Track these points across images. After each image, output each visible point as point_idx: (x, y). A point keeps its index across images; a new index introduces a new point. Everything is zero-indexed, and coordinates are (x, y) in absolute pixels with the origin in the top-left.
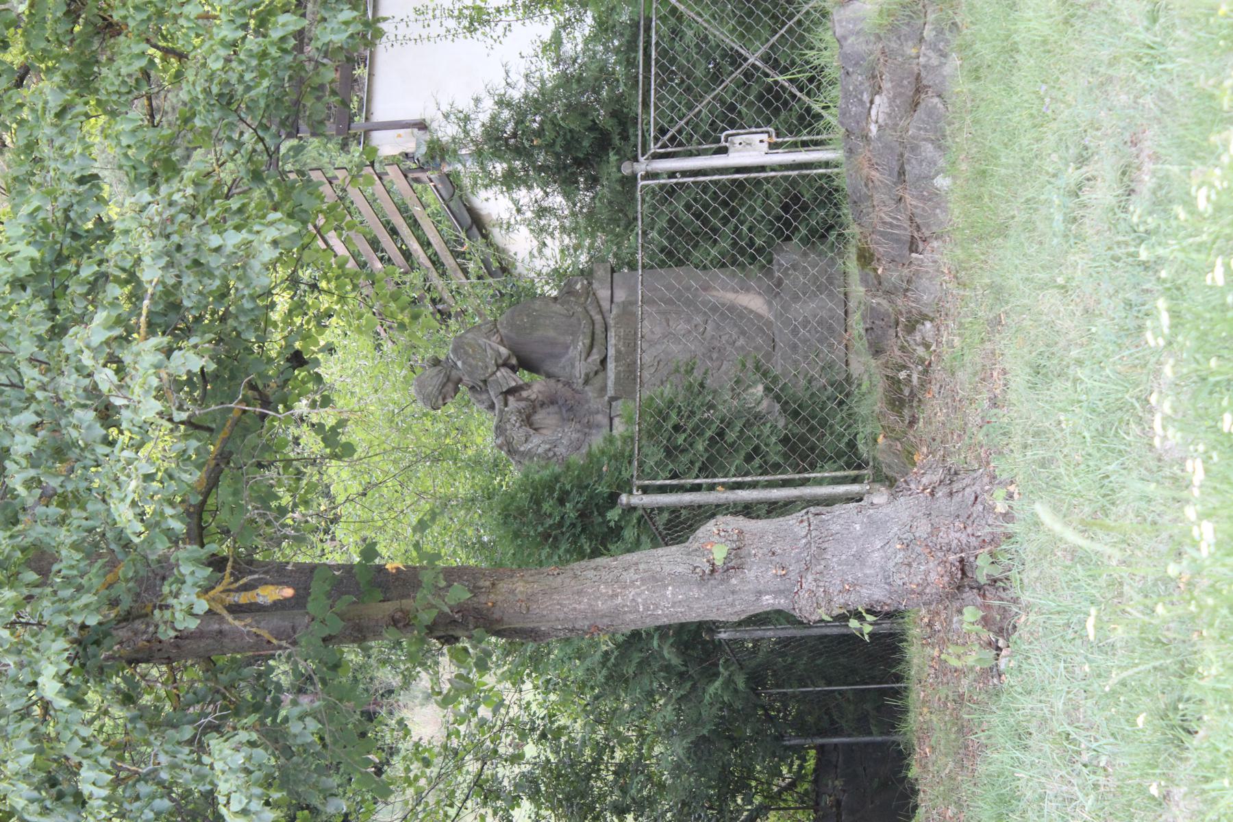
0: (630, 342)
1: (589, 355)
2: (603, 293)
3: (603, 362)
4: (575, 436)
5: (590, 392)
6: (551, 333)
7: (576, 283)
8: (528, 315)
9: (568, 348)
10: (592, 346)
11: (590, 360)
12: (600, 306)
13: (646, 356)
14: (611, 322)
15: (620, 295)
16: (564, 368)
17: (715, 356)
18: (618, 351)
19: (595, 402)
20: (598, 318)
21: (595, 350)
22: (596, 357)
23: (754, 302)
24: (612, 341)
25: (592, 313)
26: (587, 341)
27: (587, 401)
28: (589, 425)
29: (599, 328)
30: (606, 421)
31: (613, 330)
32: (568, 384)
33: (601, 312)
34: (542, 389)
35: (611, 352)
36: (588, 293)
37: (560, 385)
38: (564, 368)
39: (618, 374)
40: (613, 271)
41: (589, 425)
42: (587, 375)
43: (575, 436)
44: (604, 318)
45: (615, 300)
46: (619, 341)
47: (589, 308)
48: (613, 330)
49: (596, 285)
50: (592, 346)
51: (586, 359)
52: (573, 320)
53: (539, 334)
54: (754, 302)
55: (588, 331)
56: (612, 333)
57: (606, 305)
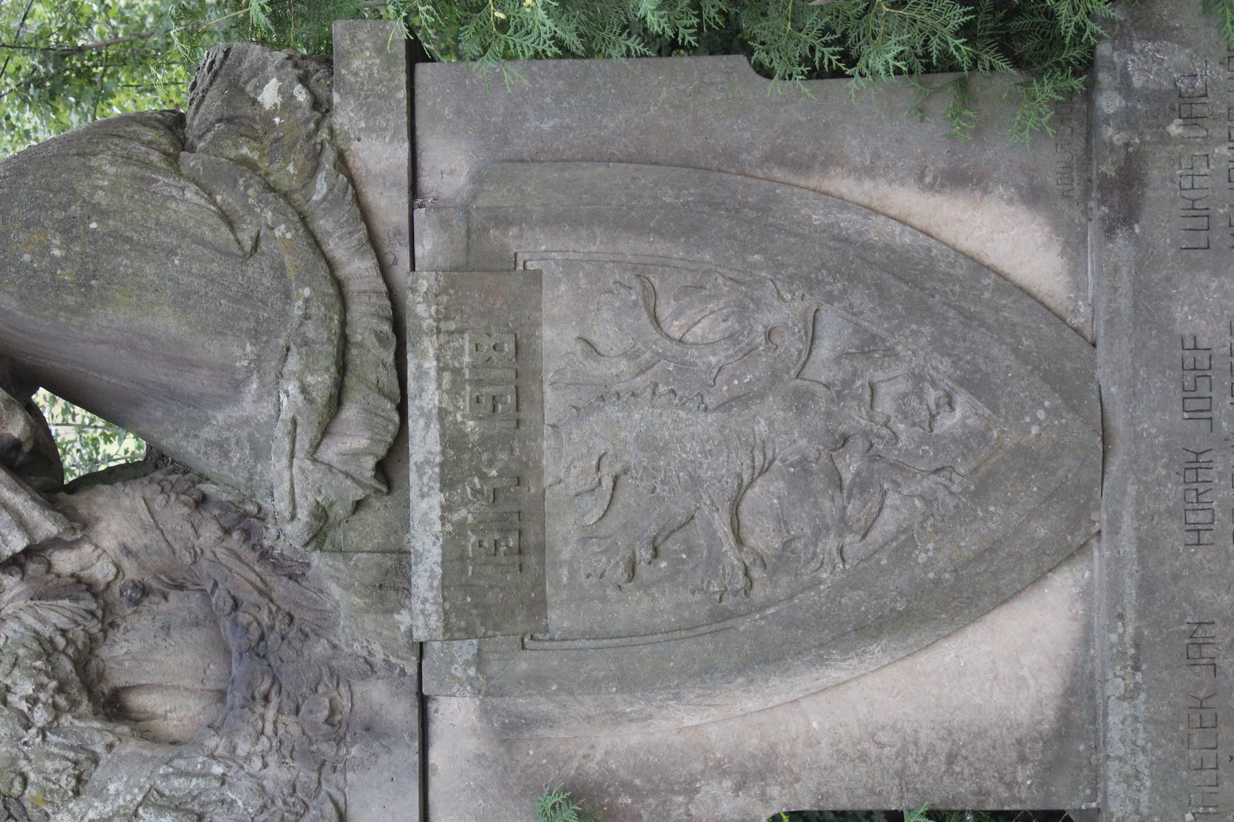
0: (508, 388)
1: (325, 431)
2: (379, 155)
3: (389, 468)
4: (276, 774)
5: (335, 584)
6: (167, 322)
7: (259, 73)
8: (67, 230)
9: (238, 386)
10: (337, 400)
11: (331, 451)
12: (365, 215)
13: (565, 461)
14: (421, 310)
15: (450, 167)
16: (222, 447)
17: (850, 467)
18: (453, 441)
19: (351, 621)
20: (359, 269)
21: (351, 412)
22: (355, 439)
23: (1010, 239)
24: (426, 395)
25: (337, 248)
26: (321, 381)
27: (323, 623)
28: (338, 728)
29: (367, 322)
30: (402, 712)
31: (429, 345)
32: (244, 522)
33: (373, 242)
34: (138, 540)
35: (424, 443)
36: (316, 157)
37: (210, 533)
38: (222, 447)
39: (453, 541)
40: (416, 53)
41: (338, 728)
42: (321, 514)
43: (276, 774)
44: (384, 270)
45: (428, 182)
46: (454, 391)
47: (323, 224)
48: (429, 345)
49: (345, 116)
50: (337, 400)
51: (316, 447)
52: (258, 273)
53: (114, 317)
54: (1010, 239)
55: (321, 334)
56: (424, 361)
57: (389, 205)
